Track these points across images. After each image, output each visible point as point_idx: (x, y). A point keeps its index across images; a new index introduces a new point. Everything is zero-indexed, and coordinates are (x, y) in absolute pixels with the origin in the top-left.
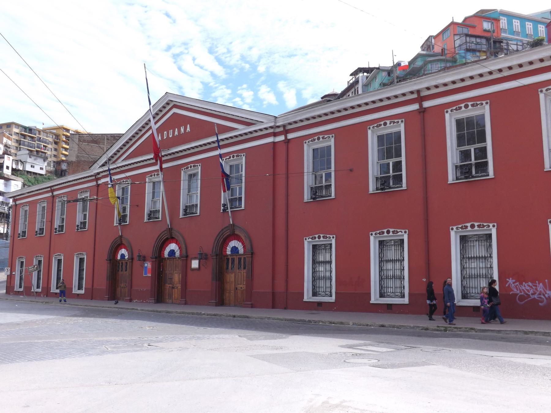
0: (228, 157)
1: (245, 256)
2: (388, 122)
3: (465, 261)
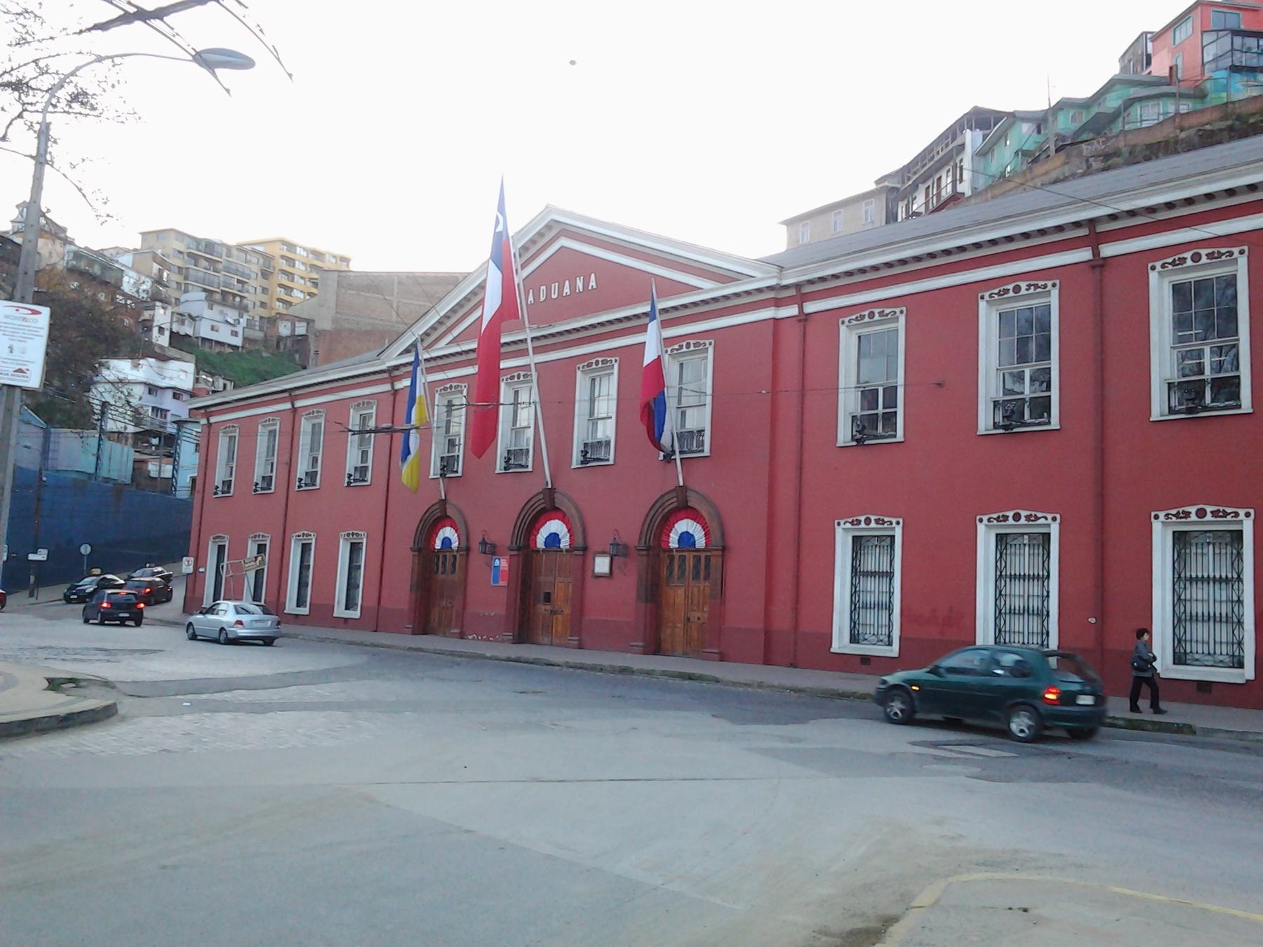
0: (677, 347)
1: (709, 554)
2: (1023, 285)
3: (1182, 586)
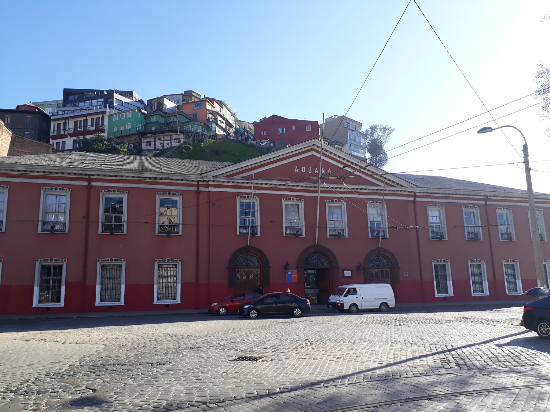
0: (372, 202)
